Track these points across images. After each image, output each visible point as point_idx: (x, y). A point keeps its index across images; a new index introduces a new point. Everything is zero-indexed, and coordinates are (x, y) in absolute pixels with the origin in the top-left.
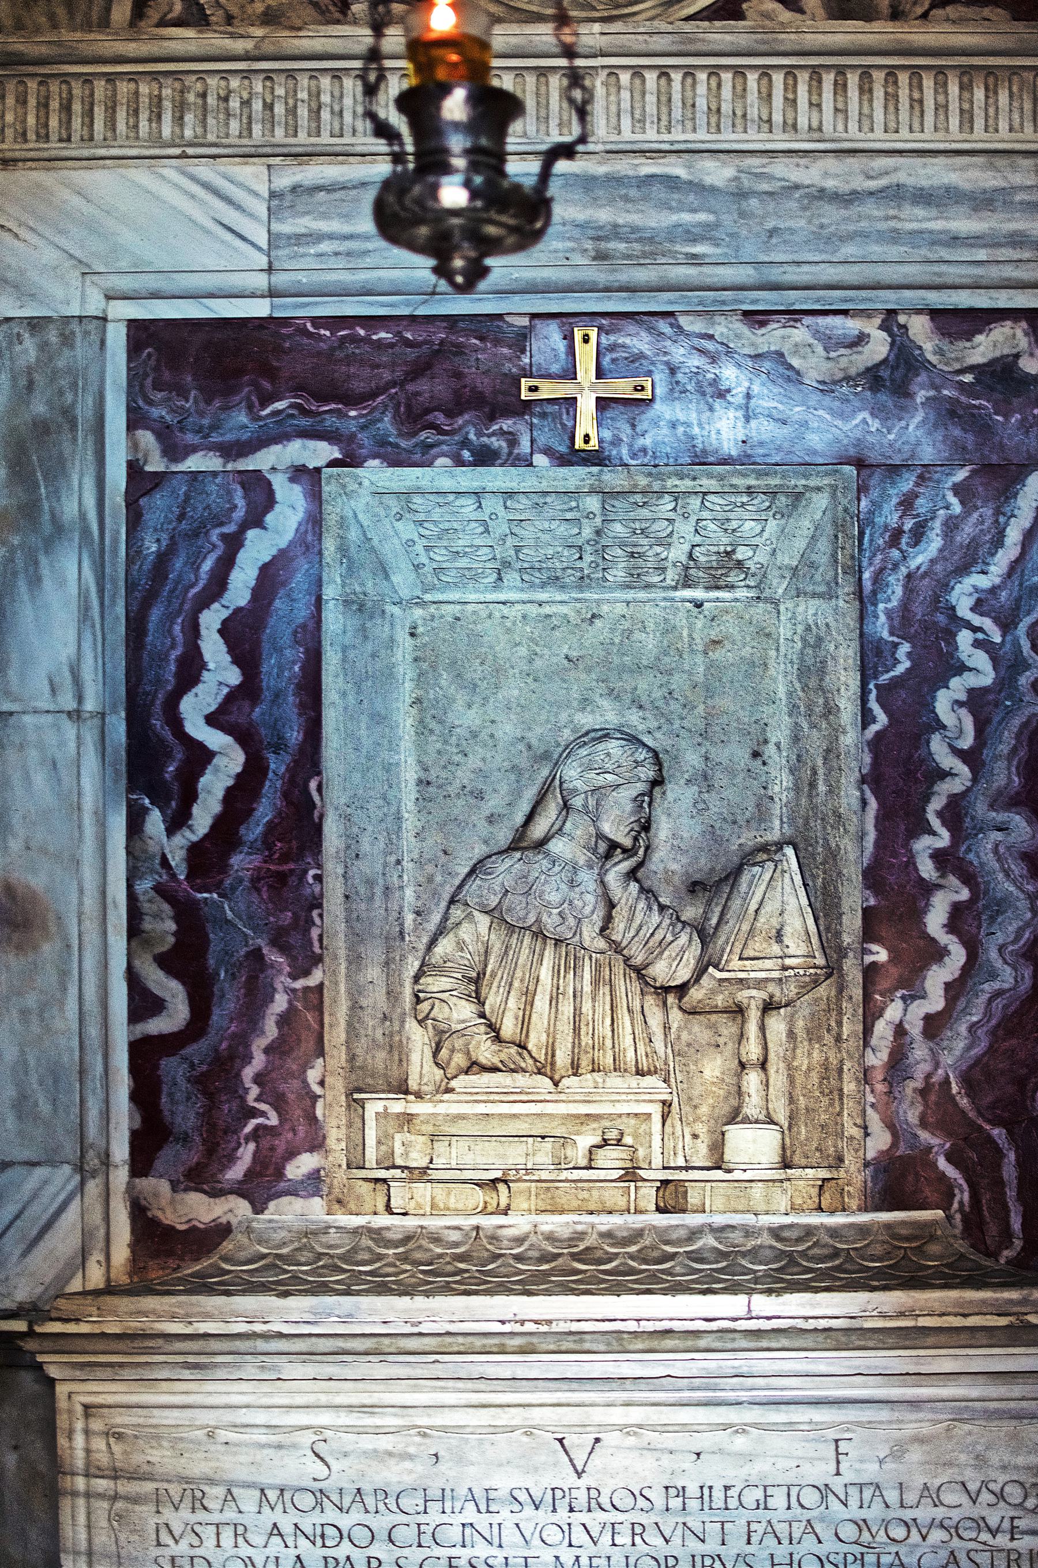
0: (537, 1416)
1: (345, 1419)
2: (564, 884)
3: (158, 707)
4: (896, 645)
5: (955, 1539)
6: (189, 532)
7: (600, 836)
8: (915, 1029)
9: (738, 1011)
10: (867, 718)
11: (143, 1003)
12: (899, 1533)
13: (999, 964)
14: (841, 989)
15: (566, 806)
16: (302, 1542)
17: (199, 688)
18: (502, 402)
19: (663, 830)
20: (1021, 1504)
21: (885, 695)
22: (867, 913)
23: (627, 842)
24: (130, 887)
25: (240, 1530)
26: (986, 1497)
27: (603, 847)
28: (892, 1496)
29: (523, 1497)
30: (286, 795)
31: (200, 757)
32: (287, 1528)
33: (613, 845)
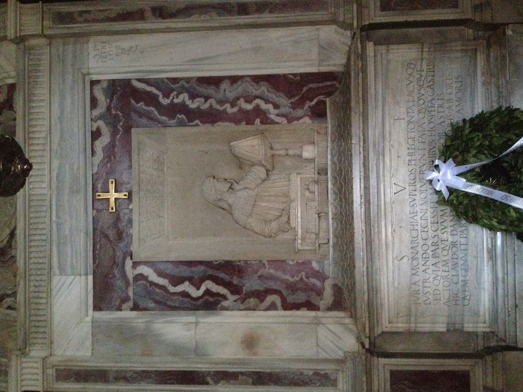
0: (388, 200)
1: (390, 252)
2: (240, 200)
3: (195, 303)
4: (178, 118)
5: (424, 86)
6: (149, 295)
7: (228, 190)
8: (277, 111)
9: (273, 156)
10: (197, 125)
12: (421, 102)
13: (260, 91)
14: (266, 130)
15: (220, 200)
16: (428, 263)
17: (190, 292)
19: (227, 175)
20: (413, 69)
21: (190, 120)
22: (247, 124)
23: (229, 185)
24: (241, 310)
25: (425, 281)
26: (411, 79)
27: (231, 190)
28: (411, 104)
29: (412, 204)
30: (218, 269)
31: (208, 292)
32: (424, 268)
33: (230, 188)
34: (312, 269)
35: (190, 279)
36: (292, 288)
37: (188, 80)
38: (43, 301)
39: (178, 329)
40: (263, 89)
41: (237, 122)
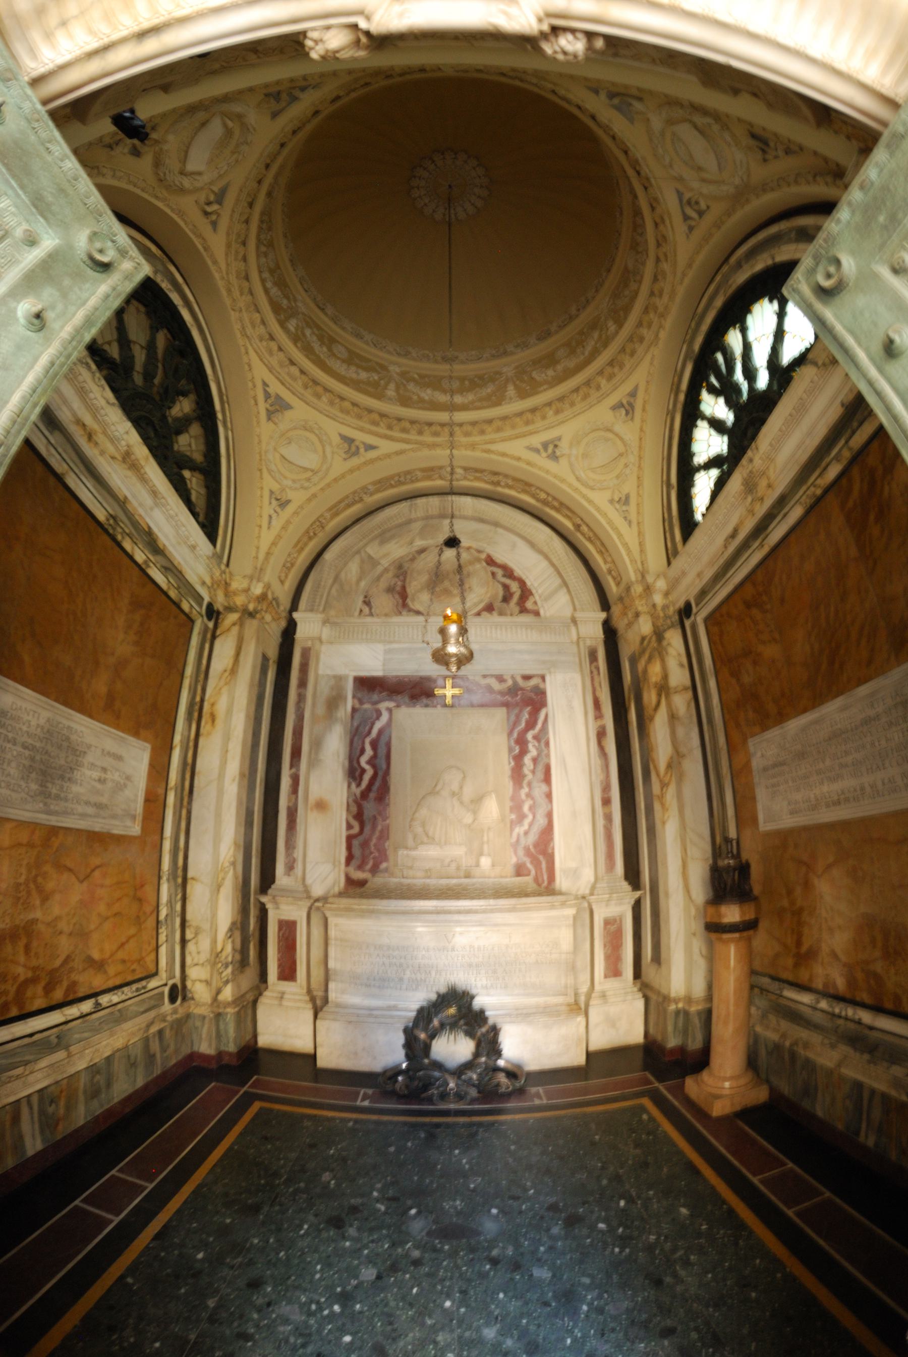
8: (522, 832)
10: (510, 763)
11: (349, 827)
18: (430, 694)
31: (363, 771)
34: (381, 863)
35: (375, 756)
36: (365, 845)
37: (548, 756)
38: (364, 636)
39: (335, 745)
40: (541, 821)
41: (513, 799)
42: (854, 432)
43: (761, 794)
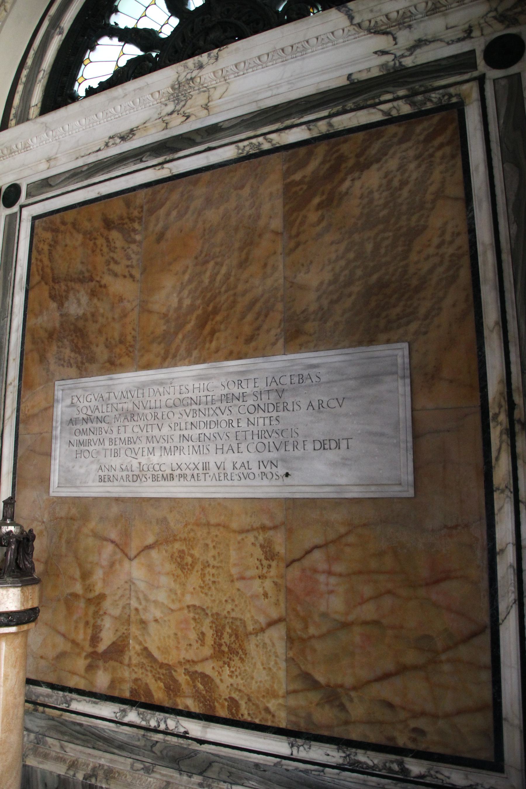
42: (345, 112)
43: (59, 450)
